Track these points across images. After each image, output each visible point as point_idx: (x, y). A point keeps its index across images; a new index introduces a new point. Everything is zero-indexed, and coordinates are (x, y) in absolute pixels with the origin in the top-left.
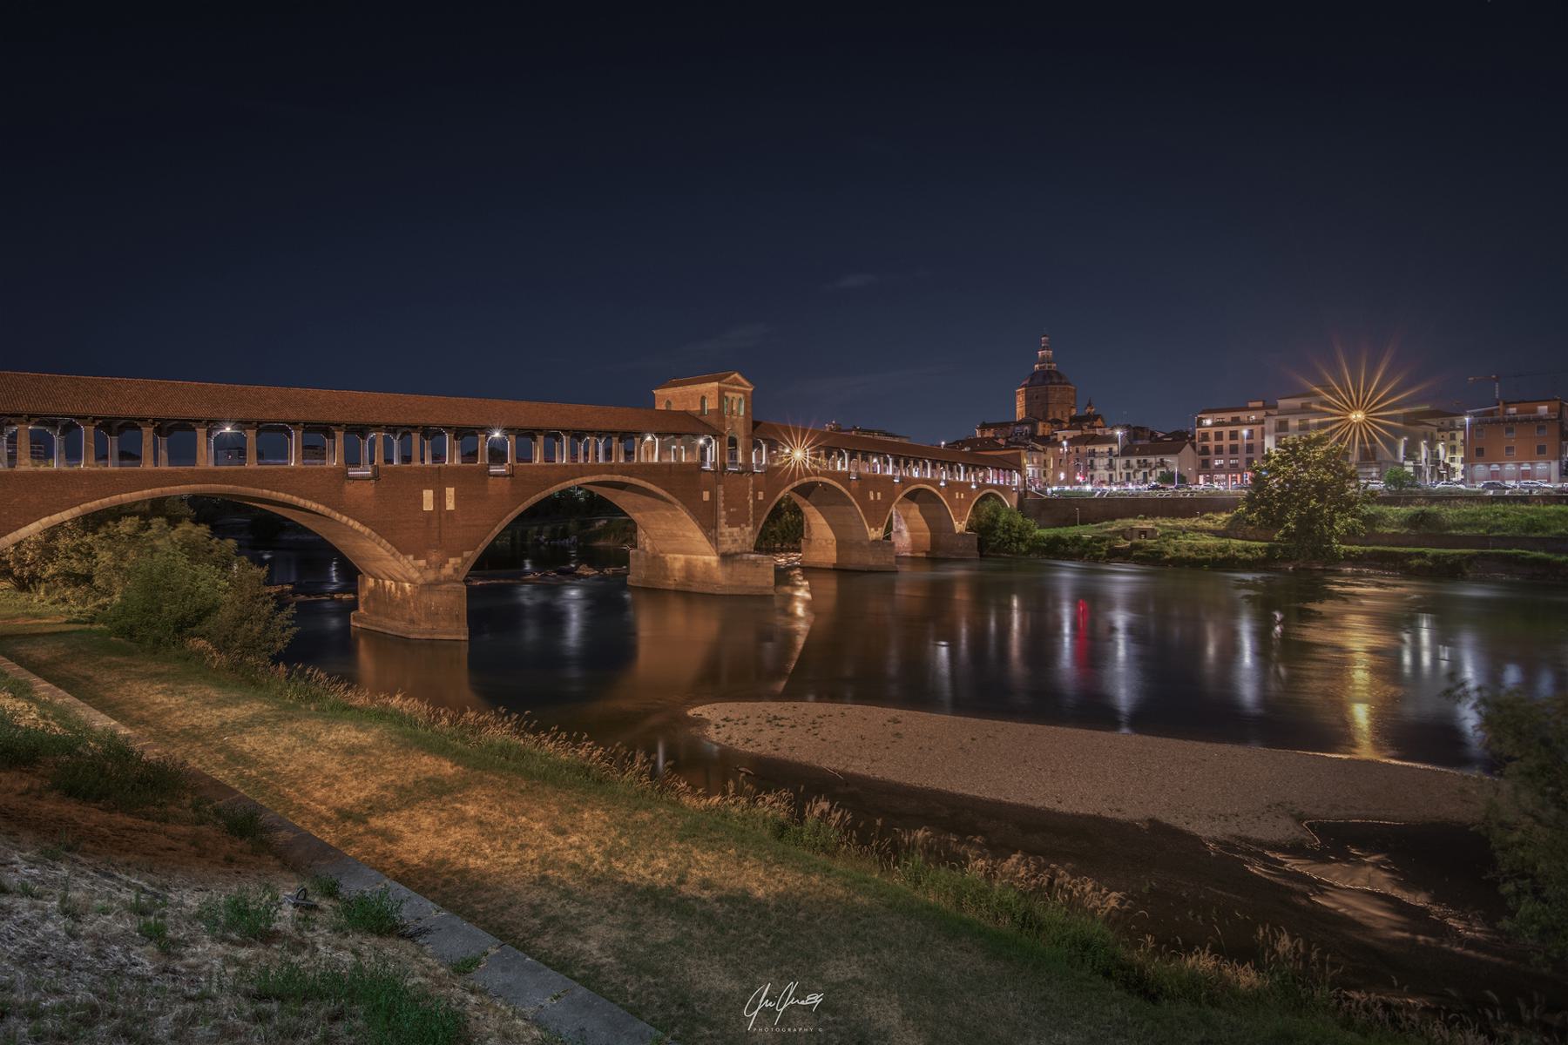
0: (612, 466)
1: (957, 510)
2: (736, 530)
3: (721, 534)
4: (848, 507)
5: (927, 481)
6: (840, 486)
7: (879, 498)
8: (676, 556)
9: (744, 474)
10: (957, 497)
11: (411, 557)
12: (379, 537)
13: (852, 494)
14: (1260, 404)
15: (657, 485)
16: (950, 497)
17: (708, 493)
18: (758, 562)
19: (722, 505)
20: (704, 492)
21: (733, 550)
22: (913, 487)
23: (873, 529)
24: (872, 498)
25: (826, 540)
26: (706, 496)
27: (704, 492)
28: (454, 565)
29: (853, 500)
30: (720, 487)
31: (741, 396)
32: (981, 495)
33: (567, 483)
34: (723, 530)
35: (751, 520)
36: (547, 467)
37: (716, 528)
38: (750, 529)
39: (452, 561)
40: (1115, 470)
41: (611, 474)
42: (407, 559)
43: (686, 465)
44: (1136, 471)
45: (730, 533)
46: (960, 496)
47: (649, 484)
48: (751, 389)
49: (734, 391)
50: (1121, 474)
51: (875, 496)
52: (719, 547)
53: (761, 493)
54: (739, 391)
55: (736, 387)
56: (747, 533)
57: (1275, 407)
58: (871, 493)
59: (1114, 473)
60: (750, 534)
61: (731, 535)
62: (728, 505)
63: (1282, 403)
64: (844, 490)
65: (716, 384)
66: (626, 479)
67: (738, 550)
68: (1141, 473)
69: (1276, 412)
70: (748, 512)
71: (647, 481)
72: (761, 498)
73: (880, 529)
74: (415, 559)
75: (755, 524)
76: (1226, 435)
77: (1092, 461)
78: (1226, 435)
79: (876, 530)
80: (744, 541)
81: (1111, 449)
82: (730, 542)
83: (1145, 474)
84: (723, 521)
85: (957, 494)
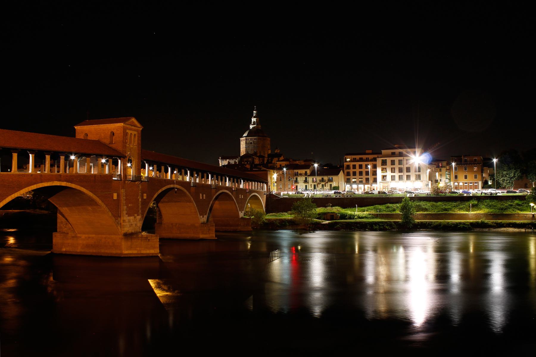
0: (60, 175)
2: (132, 218)
3: (124, 221)
4: (188, 203)
5: (227, 188)
6: (185, 191)
7: (204, 198)
8: (91, 236)
9: (137, 183)
13: (192, 196)
14: (370, 151)
16: (237, 197)
18: (148, 238)
19: (124, 202)
20: (114, 194)
21: (130, 231)
22: (221, 191)
23: (201, 217)
24: (201, 198)
25: (172, 224)
26: (115, 196)
27: (114, 194)
31: (136, 133)
32: (250, 196)
33: (32, 186)
34: (125, 218)
35: (140, 211)
36: (19, 175)
37: (120, 217)
38: (139, 217)
40: (308, 183)
41: (60, 181)
43: (95, 176)
44: (318, 184)
45: (128, 220)
46: (241, 197)
47: (82, 188)
48: (141, 129)
49: (131, 129)
50: (311, 185)
53: (145, 195)
54: (134, 130)
55: (133, 127)
56: (138, 220)
57: (381, 153)
58: (201, 195)
59: (307, 184)
61: (129, 221)
63: (384, 152)
64: (187, 193)
65: (122, 124)
66: (69, 185)
67: (133, 231)
68: (321, 185)
69: (380, 156)
70: (139, 207)
72: (145, 198)
75: (142, 214)
76: (357, 167)
77: (297, 179)
78: (357, 167)
79: (203, 217)
80: (136, 225)
81: (306, 172)
82: (128, 226)
83: (323, 186)
85: (240, 195)
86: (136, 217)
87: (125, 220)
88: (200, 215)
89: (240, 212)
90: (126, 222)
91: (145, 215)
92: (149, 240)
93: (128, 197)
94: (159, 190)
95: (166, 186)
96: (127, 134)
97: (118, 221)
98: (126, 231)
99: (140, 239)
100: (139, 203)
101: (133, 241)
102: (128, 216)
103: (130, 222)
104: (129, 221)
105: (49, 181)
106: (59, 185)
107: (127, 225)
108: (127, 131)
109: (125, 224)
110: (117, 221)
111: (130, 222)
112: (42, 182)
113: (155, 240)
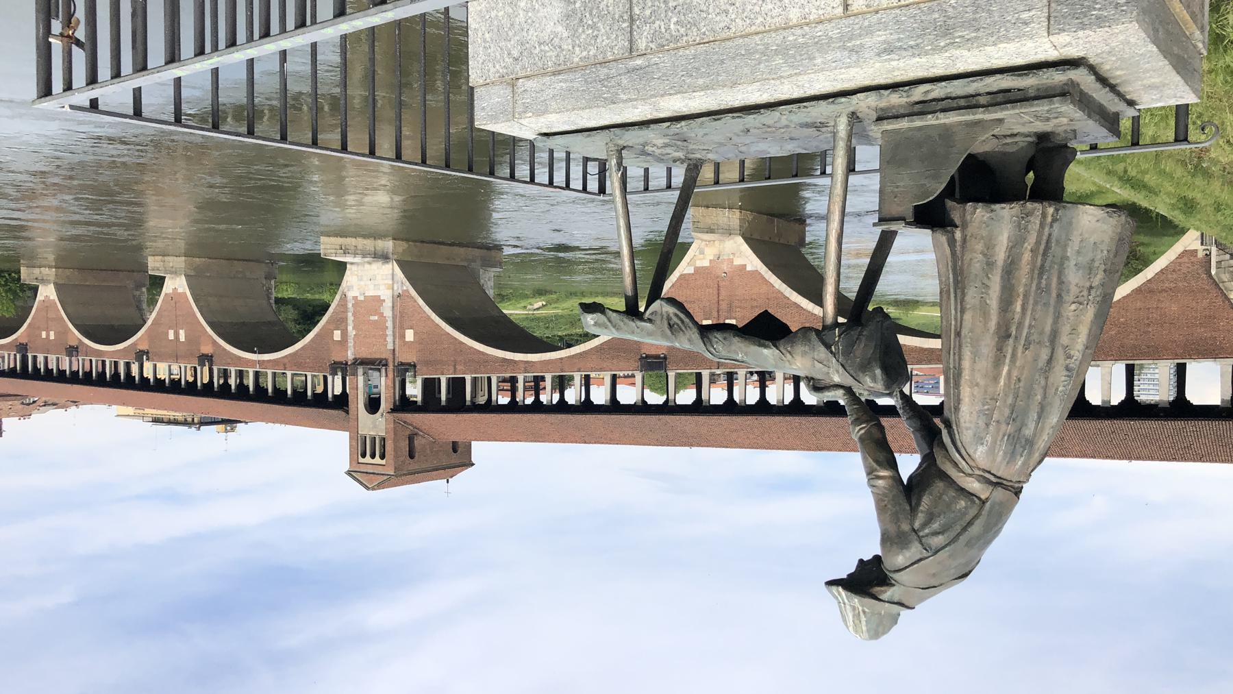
1: (51, 315)
2: (371, 293)
4: (215, 320)
10: (52, 333)
11: (749, 268)
12: (782, 291)
15: (471, 348)
16: (64, 332)
17: (407, 339)
20: (412, 340)
24: (182, 334)
26: (410, 335)
28: (704, 259)
29: (209, 329)
30: (390, 347)
32: (14, 337)
33: (578, 351)
35: (350, 305)
38: (350, 295)
39: (706, 263)
42: (752, 265)
47: (481, 350)
51: (177, 335)
52: (391, 272)
58: (182, 338)
60: (352, 287)
61: (376, 286)
62: (381, 325)
67: (367, 266)
70: (354, 314)
71: (483, 353)
73: (171, 292)
74: (746, 265)
82: (379, 277)
84: (388, 304)
86: (361, 295)
87: (388, 289)
88: (185, 293)
89: (52, 298)
90: (385, 284)
91: (338, 297)
92: (341, 249)
93: (381, 333)
94: (302, 348)
95: (283, 358)
96: (383, 457)
97: (402, 286)
98: (384, 267)
99: (359, 252)
100: (353, 321)
101: (373, 249)
102: (380, 296)
103: (375, 285)
104: (376, 286)
105: (549, 360)
106: (529, 355)
107: (383, 279)
108: (383, 462)
109: (386, 282)
110: (405, 288)
111: (375, 285)
112: (560, 359)
113: (328, 247)
